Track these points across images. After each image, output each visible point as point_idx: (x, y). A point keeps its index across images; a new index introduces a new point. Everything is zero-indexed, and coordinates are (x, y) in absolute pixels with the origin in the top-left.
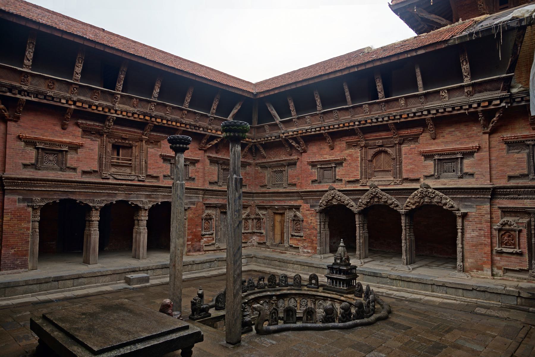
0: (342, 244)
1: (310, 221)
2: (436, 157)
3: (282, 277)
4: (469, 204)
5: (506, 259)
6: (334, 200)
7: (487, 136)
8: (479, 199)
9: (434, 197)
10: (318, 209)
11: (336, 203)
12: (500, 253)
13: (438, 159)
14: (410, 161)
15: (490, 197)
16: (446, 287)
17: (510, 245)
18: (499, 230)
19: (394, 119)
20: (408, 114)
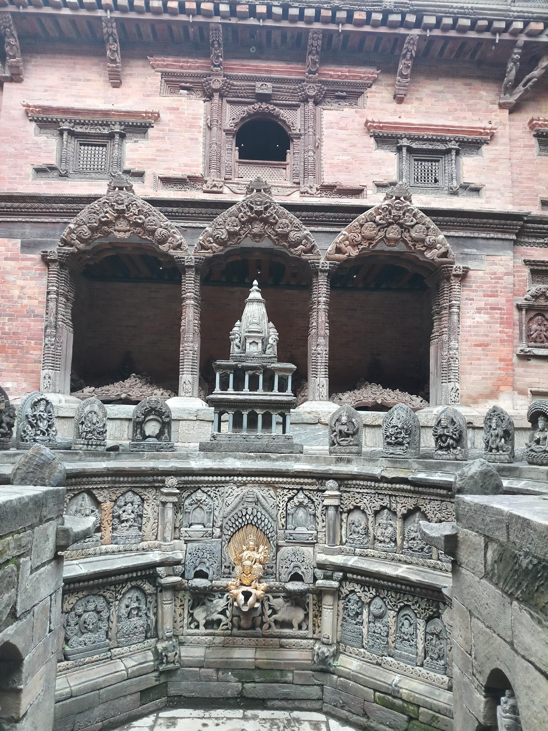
0: (255, 294)
1: (16, 292)
2: (405, 142)
3: (35, 405)
4: (474, 251)
5: (536, 370)
6: (122, 225)
7: (507, 112)
8: (492, 242)
9: (412, 227)
10: (54, 250)
11: (126, 235)
12: (525, 357)
13: (410, 150)
14: (344, 145)
15: (514, 237)
16: (474, 428)
17: (543, 342)
18: (529, 309)
19: (333, 20)
20: (369, 14)
